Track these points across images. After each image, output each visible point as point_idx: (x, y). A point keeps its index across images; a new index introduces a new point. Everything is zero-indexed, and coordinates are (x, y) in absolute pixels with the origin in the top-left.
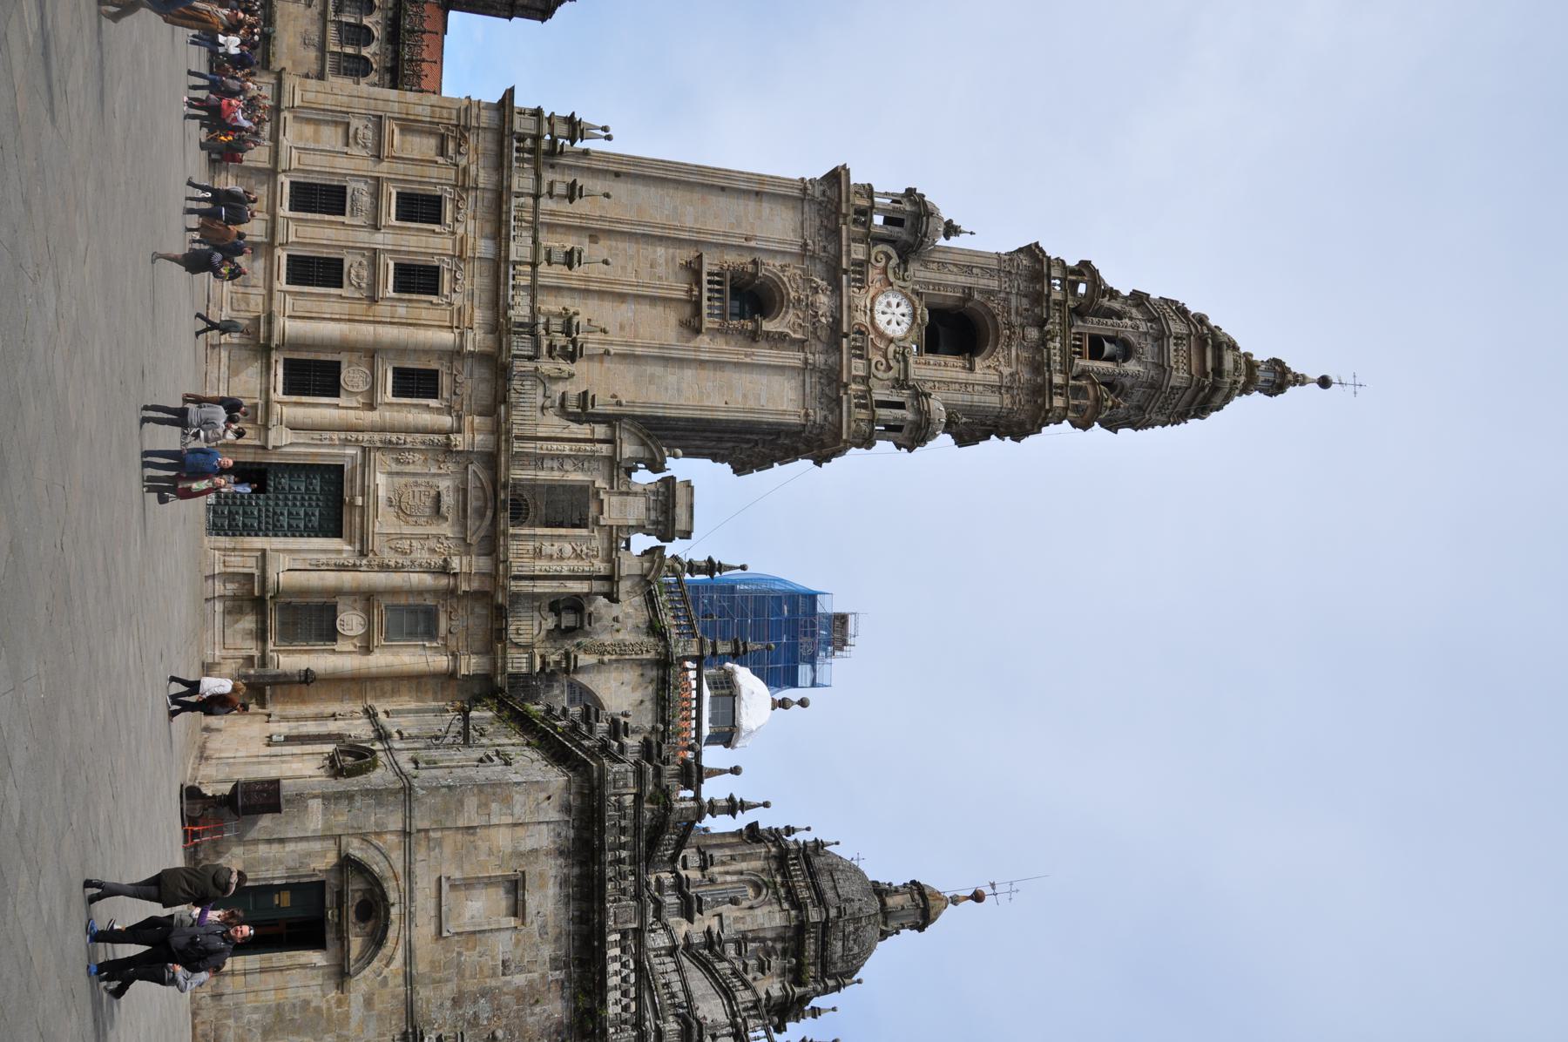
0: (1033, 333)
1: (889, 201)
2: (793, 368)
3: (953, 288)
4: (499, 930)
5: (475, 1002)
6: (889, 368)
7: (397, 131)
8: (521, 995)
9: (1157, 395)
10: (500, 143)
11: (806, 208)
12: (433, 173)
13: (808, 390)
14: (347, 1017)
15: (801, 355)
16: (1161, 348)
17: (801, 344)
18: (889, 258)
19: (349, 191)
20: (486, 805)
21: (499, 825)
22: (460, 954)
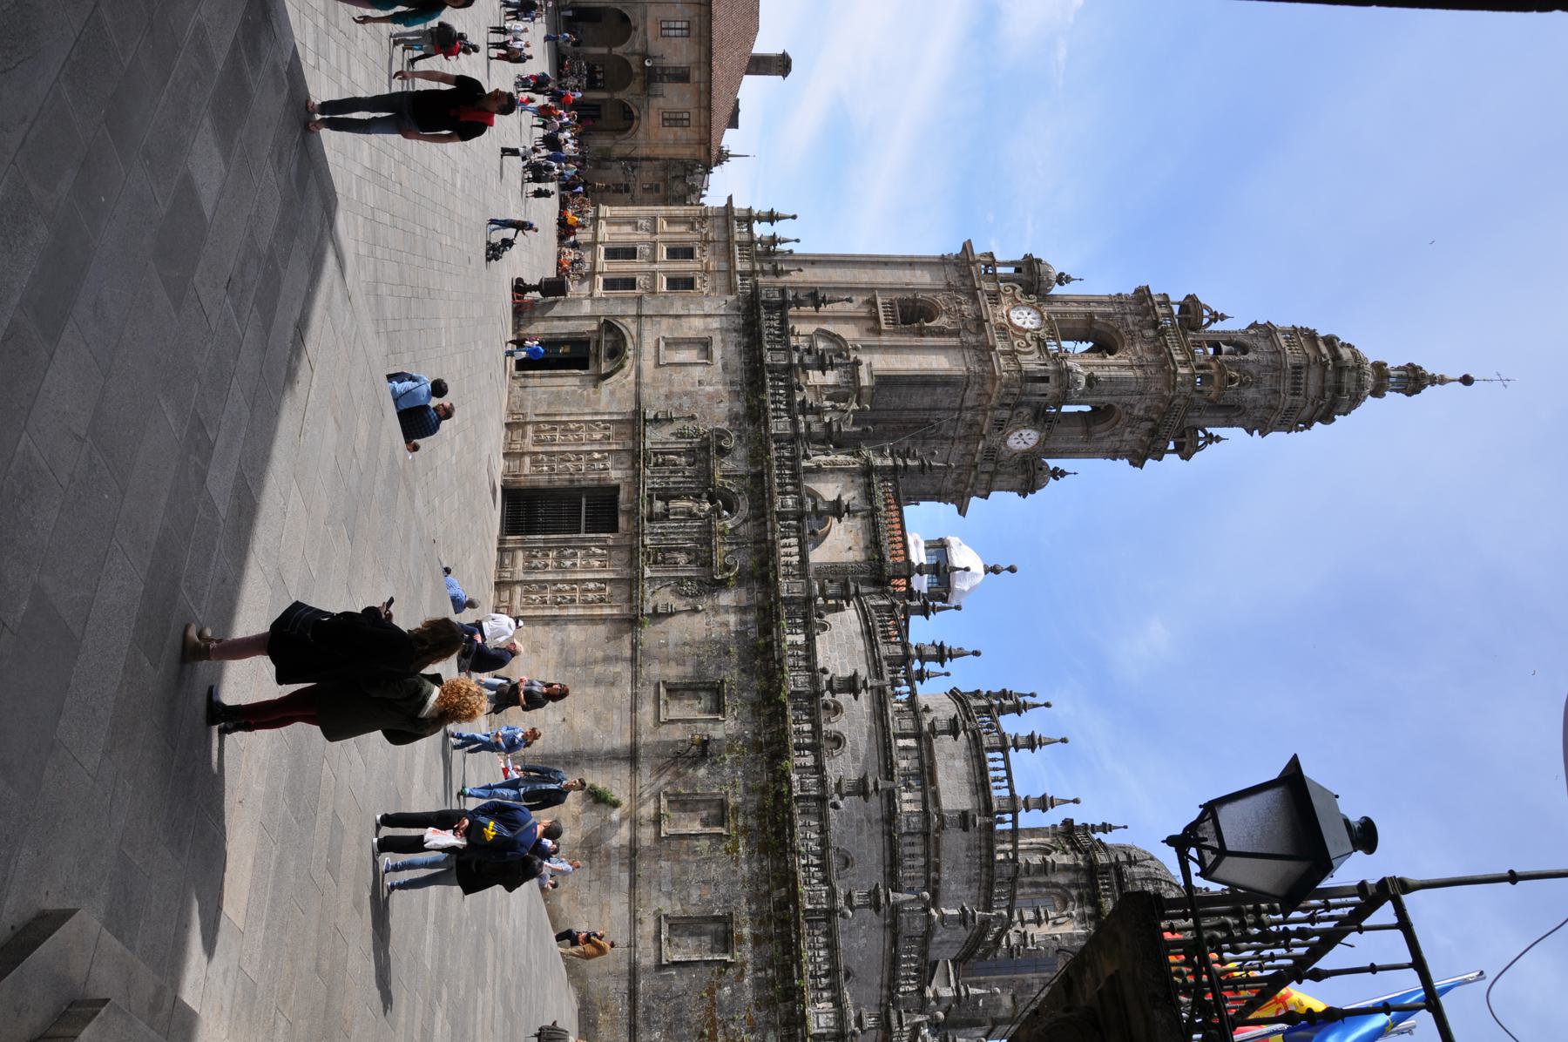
0: (1150, 333)
1: (1011, 270)
2: (954, 347)
3: (1078, 313)
4: (688, 316)
5: (680, 398)
6: (1028, 345)
7: (665, 223)
8: (710, 397)
9: (1283, 374)
10: (727, 221)
11: (947, 269)
12: (687, 237)
13: (968, 360)
14: (599, 399)
15: (958, 339)
16: (1272, 341)
17: (956, 333)
18: (1014, 289)
19: (638, 249)
20: (687, 305)
21: (695, 316)
22: (671, 375)
